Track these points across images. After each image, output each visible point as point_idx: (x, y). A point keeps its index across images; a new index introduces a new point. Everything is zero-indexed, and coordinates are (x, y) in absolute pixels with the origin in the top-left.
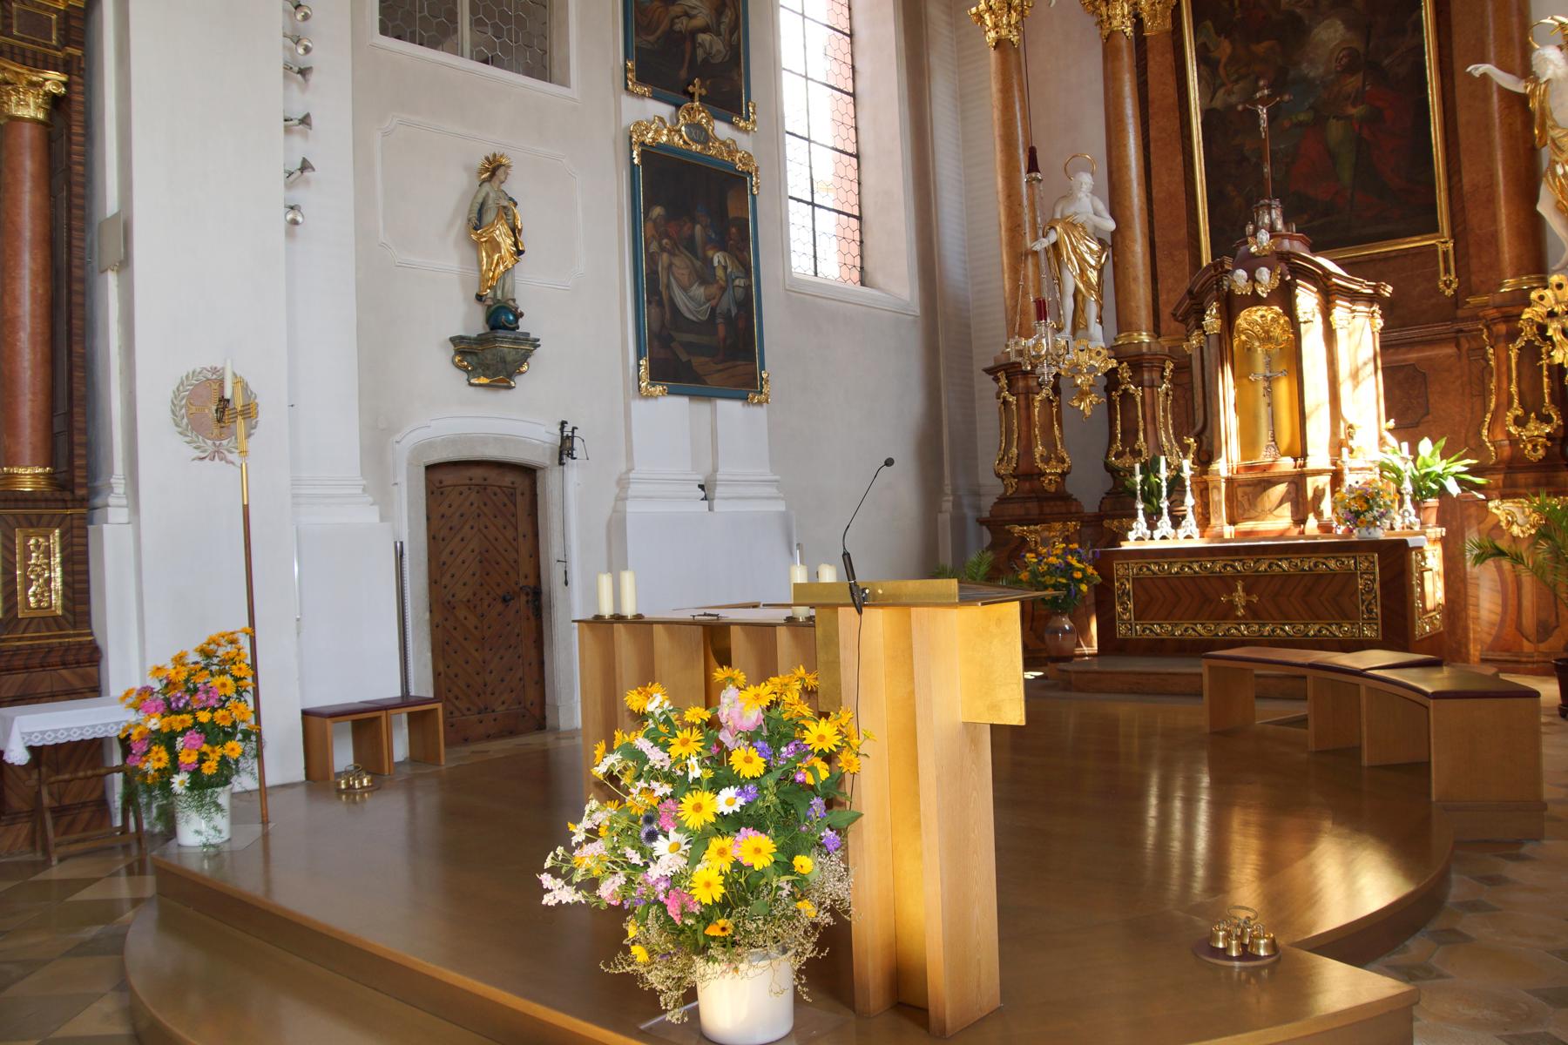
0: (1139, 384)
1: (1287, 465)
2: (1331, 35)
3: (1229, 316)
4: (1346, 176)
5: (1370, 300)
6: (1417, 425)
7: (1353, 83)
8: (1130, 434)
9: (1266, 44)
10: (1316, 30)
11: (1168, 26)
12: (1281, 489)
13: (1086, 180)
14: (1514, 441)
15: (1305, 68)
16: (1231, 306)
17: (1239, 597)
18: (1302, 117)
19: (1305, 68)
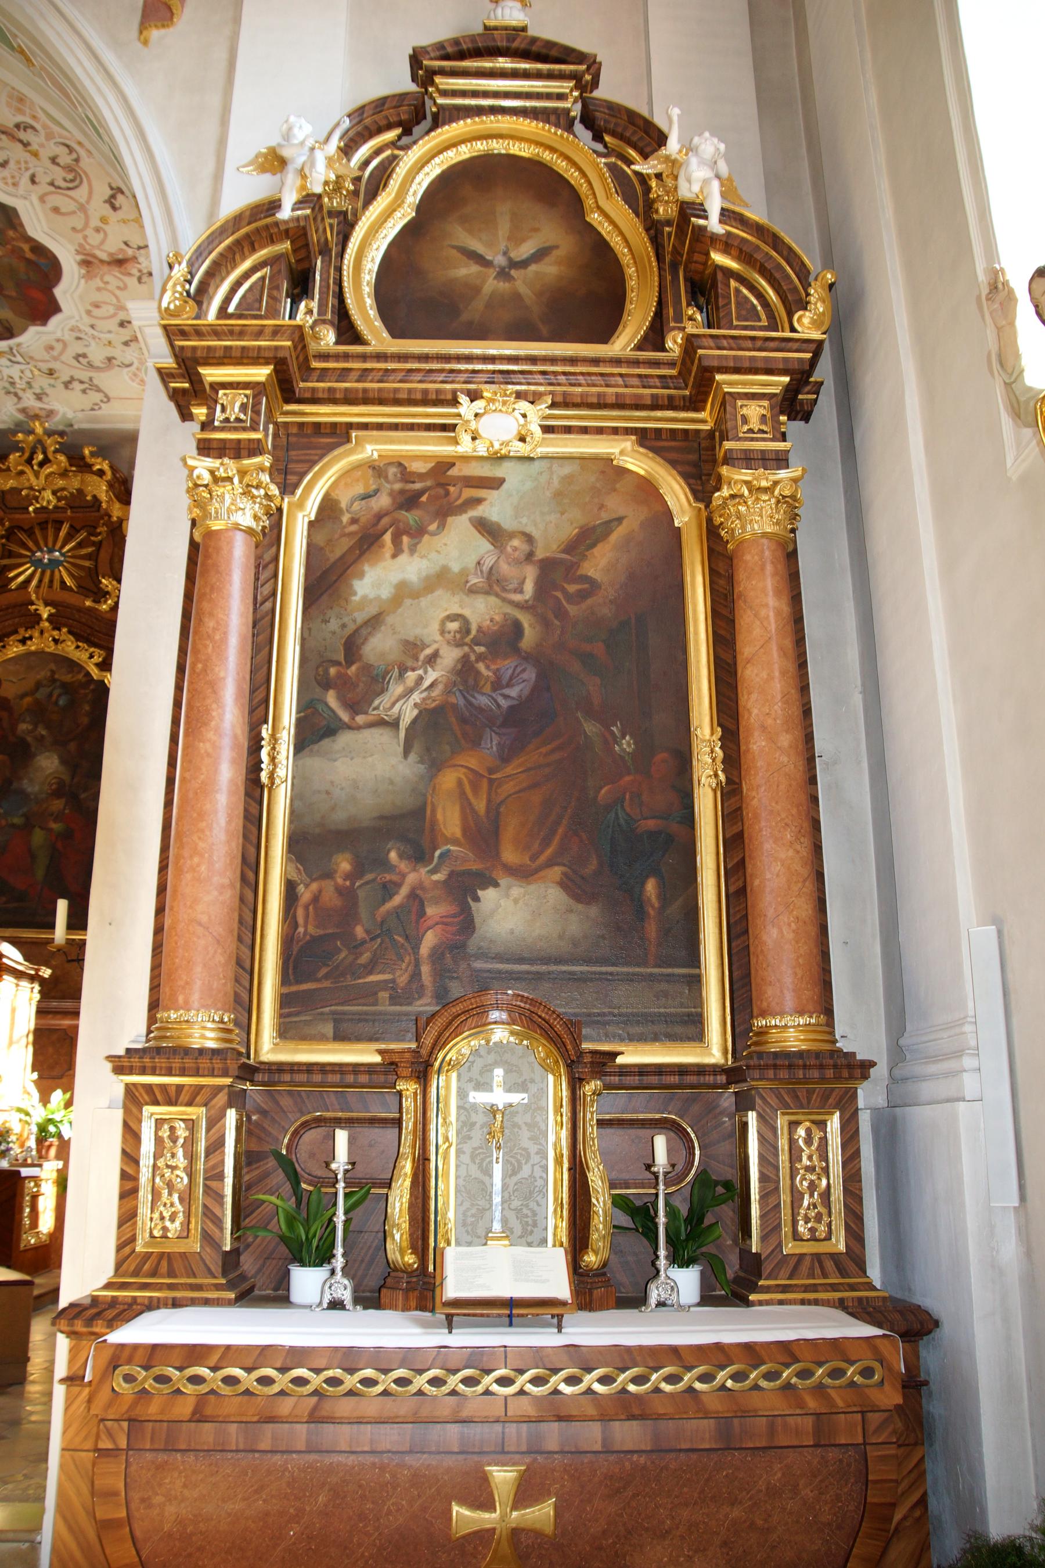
4: (40, 873)
5: (32, 979)
6: (61, 1077)
7: (58, 805)
10: (38, 758)
18: (17, 820)
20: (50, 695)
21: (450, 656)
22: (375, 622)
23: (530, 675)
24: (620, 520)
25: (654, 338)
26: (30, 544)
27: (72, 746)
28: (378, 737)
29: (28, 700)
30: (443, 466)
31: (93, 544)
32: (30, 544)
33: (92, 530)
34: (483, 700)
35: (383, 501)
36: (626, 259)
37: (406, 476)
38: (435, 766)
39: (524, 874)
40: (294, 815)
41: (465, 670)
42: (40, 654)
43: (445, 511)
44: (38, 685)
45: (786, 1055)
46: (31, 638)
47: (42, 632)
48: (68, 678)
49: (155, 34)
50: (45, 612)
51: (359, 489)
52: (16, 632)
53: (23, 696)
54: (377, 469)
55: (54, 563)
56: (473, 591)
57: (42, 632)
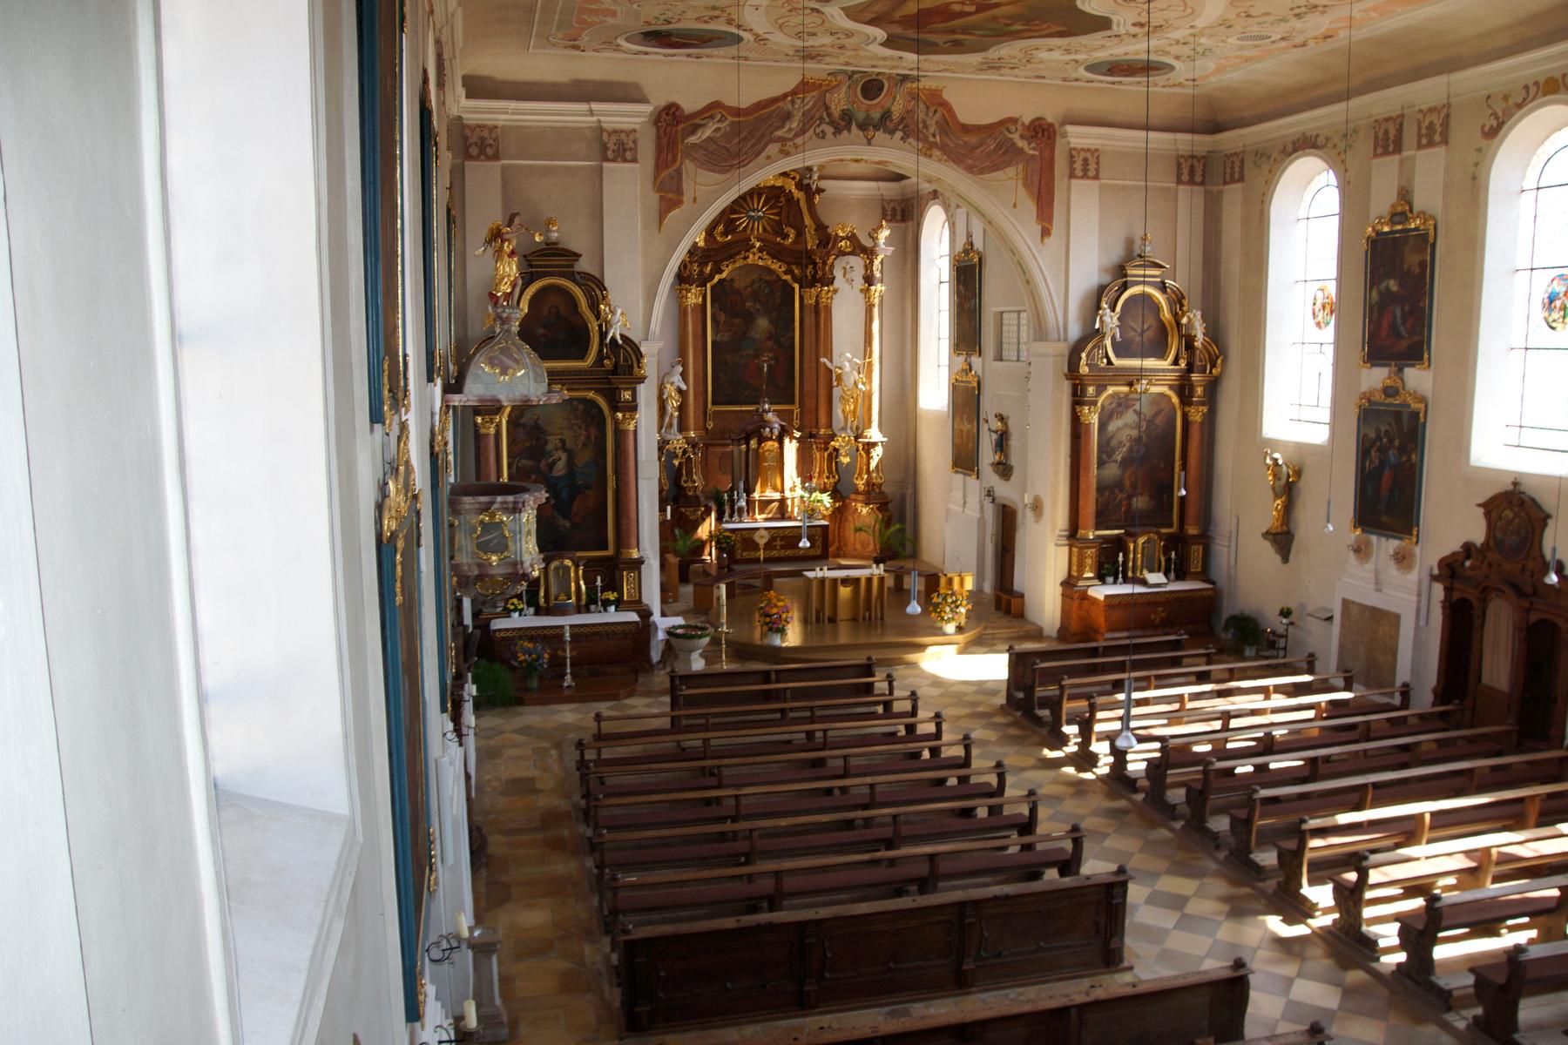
0: (694, 454)
1: (777, 496)
2: (763, 323)
3: (759, 443)
7: (770, 344)
8: (689, 473)
9: (739, 320)
11: (700, 299)
12: (775, 505)
13: (681, 369)
14: (825, 484)
15: (753, 334)
16: (762, 440)
17: (778, 543)
18: (751, 352)
19: (753, 334)
20: (760, 287)
21: (1128, 444)
22: (1113, 437)
23: (1143, 449)
24: (1163, 410)
25: (1176, 362)
26: (744, 204)
27: (774, 314)
28: (1113, 465)
29: (749, 289)
30: (1127, 395)
31: (778, 207)
32: (744, 204)
33: (777, 198)
34: (1135, 455)
35: (1114, 405)
36: (1169, 329)
37: (1119, 398)
38: (1124, 470)
39: (1141, 494)
40: (1098, 483)
41: (1131, 449)
42: (755, 267)
43: (1128, 407)
44: (753, 282)
45: (1194, 535)
46: (748, 257)
47: (754, 254)
48: (767, 278)
49: (1046, 240)
50: (758, 244)
51: (1109, 402)
52: (739, 253)
53: (747, 287)
54: (1112, 396)
55: (760, 218)
56: (1134, 428)
57: (754, 254)
